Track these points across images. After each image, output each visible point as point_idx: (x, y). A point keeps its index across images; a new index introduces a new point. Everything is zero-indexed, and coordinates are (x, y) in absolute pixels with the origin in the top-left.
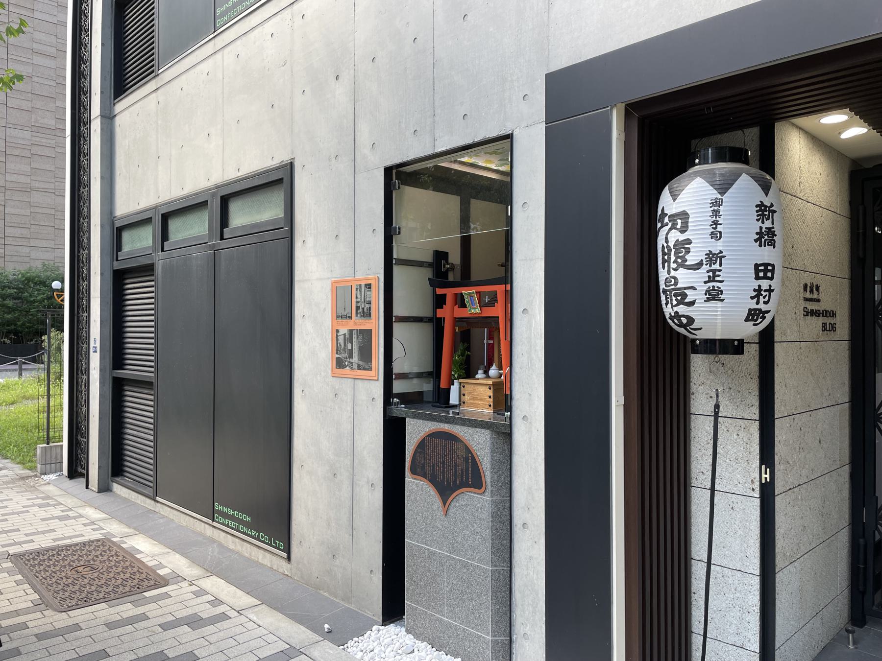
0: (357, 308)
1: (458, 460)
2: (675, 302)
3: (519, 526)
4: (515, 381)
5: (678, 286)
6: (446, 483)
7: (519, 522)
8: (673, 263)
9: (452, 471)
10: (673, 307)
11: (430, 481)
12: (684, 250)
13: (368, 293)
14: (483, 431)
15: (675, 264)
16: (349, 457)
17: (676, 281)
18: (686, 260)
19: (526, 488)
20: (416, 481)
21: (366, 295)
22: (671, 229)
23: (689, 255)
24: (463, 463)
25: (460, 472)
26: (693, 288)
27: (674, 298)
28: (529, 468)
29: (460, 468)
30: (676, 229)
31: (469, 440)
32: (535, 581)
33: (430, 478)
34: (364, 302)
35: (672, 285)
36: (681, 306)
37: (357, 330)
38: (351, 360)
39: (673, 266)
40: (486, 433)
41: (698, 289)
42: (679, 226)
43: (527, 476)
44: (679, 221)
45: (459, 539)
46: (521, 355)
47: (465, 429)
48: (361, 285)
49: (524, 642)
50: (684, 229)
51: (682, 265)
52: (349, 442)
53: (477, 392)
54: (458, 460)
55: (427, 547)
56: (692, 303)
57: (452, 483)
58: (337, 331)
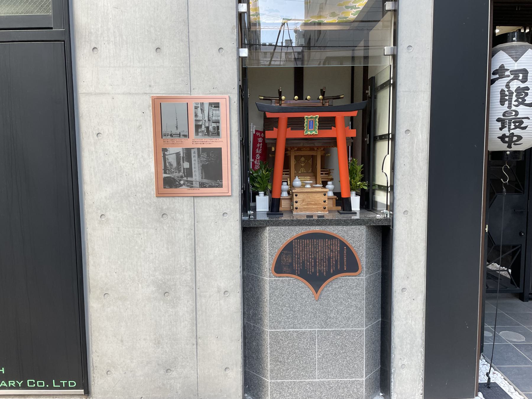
0: (198, 127)
1: (332, 254)
2: (512, 126)
3: (398, 291)
4: (396, 185)
5: (518, 117)
6: (318, 274)
7: (398, 289)
8: (515, 101)
9: (325, 263)
10: (510, 129)
11: (298, 275)
12: (524, 94)
13: (214, 112)
14: (358, 227)
15: (516, 102)
16: (189, 273)
17: (517, 113)
18: (525, 100)
19: (406, 263)
20: (281, 279)
21: (211, 114)
22: (512, 80)
23: (527, 97)
24: (337, 255)
25: (334, 262)
26: (528, 118)
27: (512, 124)
28: (409, 248)
29: (334, 259)
30: (518, 79)
31: (344, 236)
32: (413, 326)
33: (299, 273)
34: (209, 120)
35: (513, 116)
36: (518, 129)
37: (198, 149)
38: (189, 179)
39: (514, 103)
40: (361, 229)
41: (530, 119)
42: (520, 78)
43: (407, 255)
44: (521, 75)
45: (332, 315)
46: (403, 165)
47: (340, 228)
48: (202, 104)
49: (402, 371)
50: (524, 80)
51: (523, 103)
52: (188, 259)
53: (311, 199)
54: (332, 254)
55: (295, 330)
56: (525, 128)
57: (325, 273)
58: (165, 150)
